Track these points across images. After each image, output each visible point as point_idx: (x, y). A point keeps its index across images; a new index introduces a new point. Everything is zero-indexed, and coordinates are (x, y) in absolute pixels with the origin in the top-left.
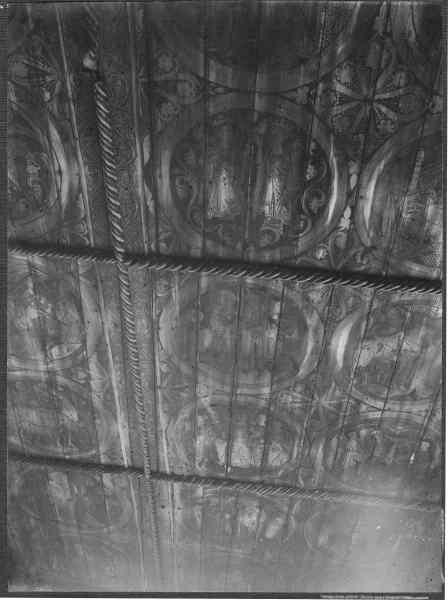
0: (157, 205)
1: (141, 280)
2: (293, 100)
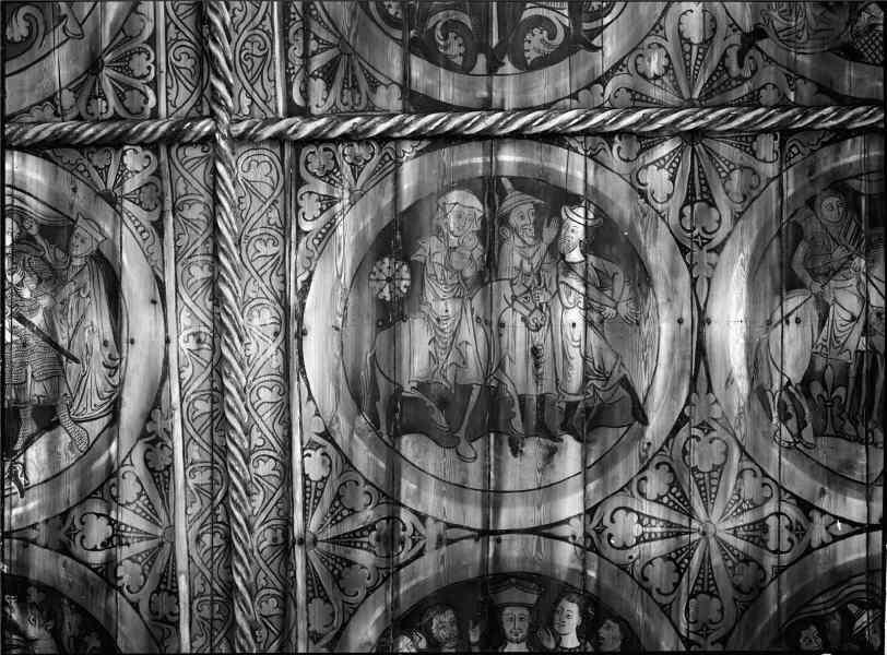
1: (267, 191)
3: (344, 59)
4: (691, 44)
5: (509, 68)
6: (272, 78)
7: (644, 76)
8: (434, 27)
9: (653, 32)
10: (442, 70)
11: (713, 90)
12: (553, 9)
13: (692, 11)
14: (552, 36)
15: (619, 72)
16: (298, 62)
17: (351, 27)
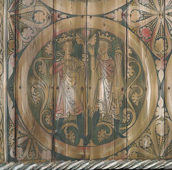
0: (17, 113)
2: (112, 19)
3: (30, 141)
4: (160, 136)
5: (92, 144)
6: (2, 147)
7: (142, 147)
8: (64, 128)
9: (146, 131)
10: (67, 144)
11: (168, 153)
12: (108, 122)
13: (160, 124)
14: (108, 132)
15: (133, 146)
16: (12, 141)
17: (33, 128)
